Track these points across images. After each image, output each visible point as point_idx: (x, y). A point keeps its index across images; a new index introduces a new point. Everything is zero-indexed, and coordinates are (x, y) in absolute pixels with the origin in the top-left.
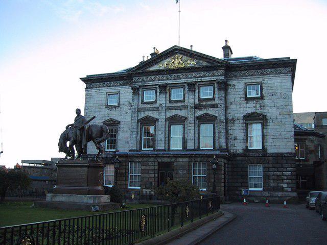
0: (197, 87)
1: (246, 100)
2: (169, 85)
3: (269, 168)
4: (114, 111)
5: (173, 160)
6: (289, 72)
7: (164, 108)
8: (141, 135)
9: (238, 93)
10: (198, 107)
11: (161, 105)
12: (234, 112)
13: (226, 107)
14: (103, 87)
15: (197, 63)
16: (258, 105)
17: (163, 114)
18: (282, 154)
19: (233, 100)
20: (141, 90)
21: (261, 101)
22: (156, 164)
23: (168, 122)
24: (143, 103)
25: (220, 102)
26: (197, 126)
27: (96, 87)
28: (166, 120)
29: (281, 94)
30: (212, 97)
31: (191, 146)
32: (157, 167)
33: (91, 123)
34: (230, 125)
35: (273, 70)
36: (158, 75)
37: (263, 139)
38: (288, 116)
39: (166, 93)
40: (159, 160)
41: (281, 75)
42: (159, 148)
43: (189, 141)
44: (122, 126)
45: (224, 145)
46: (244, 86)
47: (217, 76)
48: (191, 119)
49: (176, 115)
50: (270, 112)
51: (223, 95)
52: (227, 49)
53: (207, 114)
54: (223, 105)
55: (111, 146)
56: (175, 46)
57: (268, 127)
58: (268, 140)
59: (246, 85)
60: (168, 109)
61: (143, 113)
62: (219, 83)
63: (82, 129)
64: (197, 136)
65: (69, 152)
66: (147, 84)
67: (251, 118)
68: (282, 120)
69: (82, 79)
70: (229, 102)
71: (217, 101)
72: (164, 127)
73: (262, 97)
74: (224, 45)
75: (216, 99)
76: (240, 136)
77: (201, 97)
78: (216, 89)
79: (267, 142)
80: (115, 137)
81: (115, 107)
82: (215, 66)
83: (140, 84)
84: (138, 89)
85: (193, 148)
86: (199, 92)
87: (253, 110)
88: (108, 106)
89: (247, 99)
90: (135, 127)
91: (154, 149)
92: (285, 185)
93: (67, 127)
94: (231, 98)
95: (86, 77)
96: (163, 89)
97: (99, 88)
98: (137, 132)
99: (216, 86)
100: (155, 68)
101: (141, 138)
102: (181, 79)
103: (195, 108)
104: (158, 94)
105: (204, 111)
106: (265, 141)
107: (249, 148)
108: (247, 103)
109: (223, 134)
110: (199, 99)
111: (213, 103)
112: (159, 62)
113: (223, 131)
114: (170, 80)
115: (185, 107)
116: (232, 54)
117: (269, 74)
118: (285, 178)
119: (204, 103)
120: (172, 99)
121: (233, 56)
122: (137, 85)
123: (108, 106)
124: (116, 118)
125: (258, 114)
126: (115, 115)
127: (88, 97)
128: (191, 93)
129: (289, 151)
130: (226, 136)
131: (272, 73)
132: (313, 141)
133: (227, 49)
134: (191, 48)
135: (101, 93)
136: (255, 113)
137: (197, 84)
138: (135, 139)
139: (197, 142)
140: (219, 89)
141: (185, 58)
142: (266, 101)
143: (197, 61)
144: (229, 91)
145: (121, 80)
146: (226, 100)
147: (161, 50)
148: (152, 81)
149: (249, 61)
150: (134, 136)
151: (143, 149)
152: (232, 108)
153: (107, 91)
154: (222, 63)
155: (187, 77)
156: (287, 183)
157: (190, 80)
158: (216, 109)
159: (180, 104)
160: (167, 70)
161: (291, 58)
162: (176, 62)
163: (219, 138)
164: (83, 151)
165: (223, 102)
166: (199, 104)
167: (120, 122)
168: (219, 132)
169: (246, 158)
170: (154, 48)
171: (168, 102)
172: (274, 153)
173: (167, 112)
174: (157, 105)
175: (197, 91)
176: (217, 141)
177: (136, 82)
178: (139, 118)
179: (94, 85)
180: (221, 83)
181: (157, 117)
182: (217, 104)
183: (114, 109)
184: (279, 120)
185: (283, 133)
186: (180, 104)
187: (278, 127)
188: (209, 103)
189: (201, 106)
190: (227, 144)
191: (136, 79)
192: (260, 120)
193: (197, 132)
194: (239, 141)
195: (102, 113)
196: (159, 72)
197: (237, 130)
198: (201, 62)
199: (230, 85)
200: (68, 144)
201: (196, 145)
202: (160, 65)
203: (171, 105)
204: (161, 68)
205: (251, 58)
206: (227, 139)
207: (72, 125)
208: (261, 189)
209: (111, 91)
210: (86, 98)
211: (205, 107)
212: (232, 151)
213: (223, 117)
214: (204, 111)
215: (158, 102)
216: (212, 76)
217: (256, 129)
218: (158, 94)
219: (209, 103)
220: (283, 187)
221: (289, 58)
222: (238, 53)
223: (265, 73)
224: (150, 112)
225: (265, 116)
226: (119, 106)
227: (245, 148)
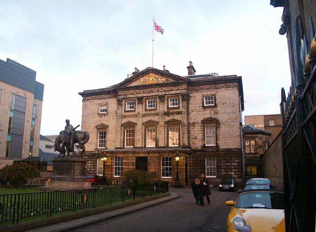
0: (166, 98)
1: (203, 108)
3: (221, 160)
5: (147, 155)
6: (236, 86)
8: (124, 136)
10: (167, 114)
11: (138, 113)
12: (195, 118)
13: (188, 114)
14: (96, 99)
16: (213, 112)
17: (140, 119)
18: (230, 150)
20: (123, 101)
21: (215, 109)
22: (134, 158)
23: (144, 126)
24: (126, 111)
25: (183, 110)
26: (166, 128)
27: (90, 100)
28: (143, 124)
29: (230, 102)
30: (177, 106)
31: (161, 144)
32: (134, 161)
33: (76, 130)
34: (191, 128)
36: (136, 89)
37: (216, 138)
39: (143, 103)
40: (136, 155)
42: (138, 146)
43: (160, 141)
44: (110, 128)
45: (186, 143)
48: (162, 123)
49: (150, 120)
50: (221, 117)
51: (186, 104)
52: (191, 68)
54: (186, 113)
56: (150, 67)
58: (221, 139)
59: (203, 96)
60: (144, 116)
62: (183, 95)
63: (70, 134)
64: (166, 136)
65: (62, 152)
66: (128, 96)
67: (207, 122)
68: (232, 123)
69: (80, 94)
70: (190, 109)
71: (180, 110)
73: (216, 106)
74: (188, 65)
75: (181, 108)
76: (200, 136)
78: (181, 100)
81: (105, 115)
83: (123, 97)
84: (122, 101)
85: (163, 145)
86: (168, 103)
87: (209, 116)
88: (99, 114)
89: (204, 107)
91: (134, 147)
92: (233, 173)
93: (60, 133)
94: (191, 107)
95: (82, 92)
96: (140, 100)
99: (180, 98)
100: (134, 84)
101: (124, 138)
103: (165, 115)
104: (137, 104)
105: (171, 117)
106: (218, 139)
107: (206, 145)
109: (186, 135)
110: (168, 108)
111: (178, 110)
113: (186, 132)
115: (157, 114)
116: (195, 72)
117: (220, 88)
118: (233, 168)
119: (172, 111)
120: (147, 108)
121: (196, 74)
122: (121, 97)
123: (99, 114)
124: (105, 123)
125: (212, 118)
126: (104, 121)
127: (84, 108)
128: (161, 103)
129: (236, 147)
130: (188, 136)
131: (223, 87)
132: (261, 138)
133: (191, 68)
134: (164, 68)
135: (95, 105)
136: (211, 118)
138: (119, 140)
139: (166, 141)
140: (183, 100)
141: (157, 76)
142: (218, 109)
144: (191, 101)
146: (188, 108)
147: (141, 68)
148: (132, 94)
150: (119, 137)
151: (125, 147)
152: (192, 115)
154: (184, 80)
155: (158, 91)
156: (234, 172)
157: (160, 94)
158: (181, 115)
159: (153, 112)
160: (143, 86)
161: (238, 76)
162: (151, 79)
163: (183, 138)
164: (71, 150)
166: (168, 111)
167: (108, 126)
168: (183, 133)
170: (136, 68)
172: (224, 149)
173: (144, 118)
174: (136, 113)
175: (166, 102)
176: (181, 141)
179: (89, 98)
180: (184, 95)
182: (181, 112)
185: (232, 133)
186: (153, 112)
187: (227, 128)
188: (175, 111)
190: (189, 143)
191: (120, 93)
193: (166, 133)
194: (198, 140)
195: (95, 119)
196: (137, 87)
197: (197, 131)
199: (191, 97)
200: (61, 145)
201: (166, 143)
203: (147, 113)
205: (209, 75)
206: (189, 138)
207: (64, 131)
208: (215, 177)
210: (83, 108)
211: (172, 114)
212: (193, 148)
213: (185, 122)
214: (171, 117)
216: (178, 90)
217: (210, 132)
218: (137, 104)
219: (175, 111)
220: (231, 175)
222: (200, 71)
227: (203, 145)
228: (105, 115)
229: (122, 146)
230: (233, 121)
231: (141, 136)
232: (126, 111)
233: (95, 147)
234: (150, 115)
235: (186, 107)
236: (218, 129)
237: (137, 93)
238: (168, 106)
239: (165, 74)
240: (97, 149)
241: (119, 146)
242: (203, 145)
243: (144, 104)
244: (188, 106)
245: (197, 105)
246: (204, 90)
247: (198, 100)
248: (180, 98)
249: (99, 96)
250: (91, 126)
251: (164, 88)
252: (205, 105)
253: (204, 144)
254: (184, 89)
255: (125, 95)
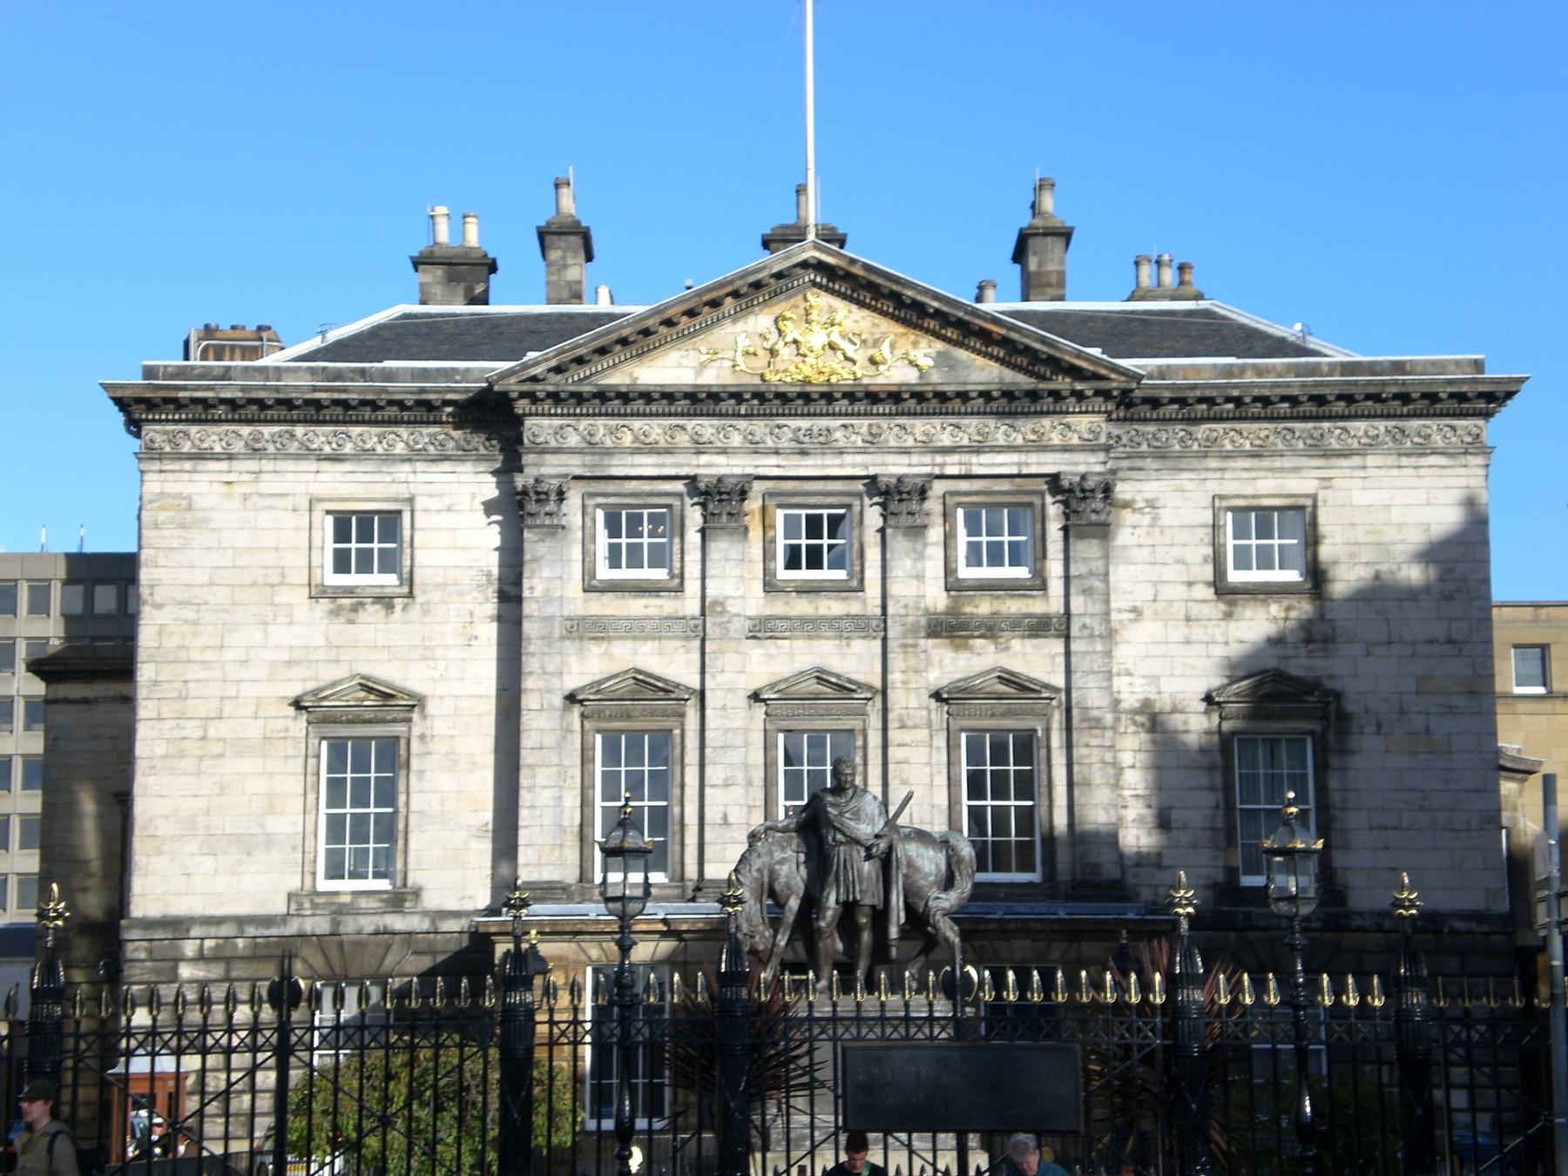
0: (933, 505)
2: (758, 487)
4: (372, 625)
7: (739, 626)
9: (1177, 552)
13: (1110, 635)
14: (282, 455)
15: (941, 359)
19: (1148, 593)
20: (574, 501)
26: (940, 741)
27: (230, 457)
35: (1382, 425)
38: (1462, 702)
39: (746, 529)
41: (1432, 460)
46: (1207, 517)
47: (1066, 449)
51: (1098, 565)
53: (1008, 678)
54: (1098, 629)
55: (361, 856)
57: (1355, 762)
60: (762, 629)
61: (596, 649)
72: (739, 741)
75: (1056, 587)
77: (965, 572)
79: (1347, 847)
80: (387, 794)
82: (1056, 395)
83: (575, 465)
84: (561, 495)
90: (550, 740)
97: (252, 465)
98: (563, 772)
101: (586, 803)
102: (841, 452)
103: (929, 636)
104: (693, 537)
108: (1228, 616)
110: (953, 585)
111: (1036, 606)
112: (692, 335)
114: (777, 452)
123: (319, 593)
124: (390, 673)
128: (898, 543)
131: (1371, 445)
137: (939, 487)
143: (939, 346)
144: (1123, 537)
145: (428, 423)
148: (653, 450)
149: (1242, 370)
153: (319, 489)
154: (1096, 377)
155: (873, 443)
159: (832, 607)
165: (1098, 608)
166: (952, 611)
167: (418, 702)
169: (1232, 936)
171: (758, 586)
173: (756, 651)
175: (935, 533)
177: (543, 450)
178: (572, 683)
179: (213, 437)
181: (695, 683)
183: (373, 612)
184: (1418, 723)
188: (1014, 606)
189: (964, 626)
192: (1306, 715)
195: (282, 635)
196: (701, 401)
198: (962, 354)
199: (1127, 505)
202: (704, 343)
203: (778, 607)
204: (713, 377)
209: (346, 490)
211: (991, 629)
215: (692, 586)
218: (693, 537)
219: (1014, 606)
221: (1478, 366)
223: (1335, 444)
224: (648, 647)
225: (1338, 696)
226: (411, 595)
227: (1221, 878)
228: (385, 601)
229: (570, 875)
230: (1451, 711)
231: (737, 792)
232: (592, 587)
233: (294, 883)
234: (811, 627)
235: (1097, 584)
236: (1334, 761)
237: (700, 447)
238: (949, 570)
239: (938, 314)
240: (315, 893)
241: (548, 874)
242: (1221, 877)
243: (756, 533)
244: (1107, 574)
245: (1171, 573)
246: (1227, 456)
247: (1181, 537)
248: (1054, 510)
249: (321, 436)
250: (248, 690)
251: (920, 426)
252: (1235, 576)
253: (1232, 873)
254: (1088, 447)
255: (591, 447)
